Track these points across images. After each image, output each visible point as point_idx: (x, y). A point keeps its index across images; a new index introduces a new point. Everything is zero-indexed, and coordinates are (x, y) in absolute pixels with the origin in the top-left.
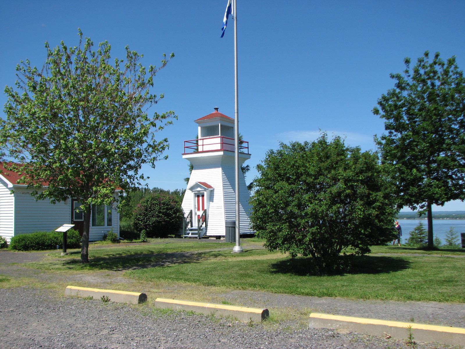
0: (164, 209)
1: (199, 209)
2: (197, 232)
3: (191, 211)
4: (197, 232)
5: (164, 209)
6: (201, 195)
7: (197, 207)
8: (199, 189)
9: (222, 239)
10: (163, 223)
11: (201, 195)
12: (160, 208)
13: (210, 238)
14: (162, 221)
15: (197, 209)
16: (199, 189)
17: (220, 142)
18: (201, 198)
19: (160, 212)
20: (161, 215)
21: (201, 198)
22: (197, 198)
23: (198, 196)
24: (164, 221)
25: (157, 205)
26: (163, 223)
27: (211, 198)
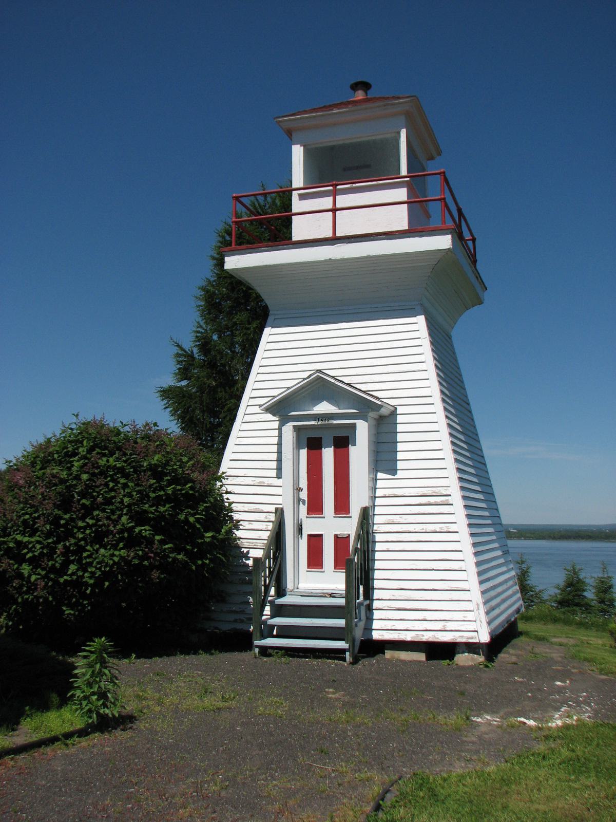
0: (158, 501)
1: (315, 507)
2: (341, 623)
3: (280, 513)
4: (341, 623)
5: (158, 501)
6: (328, 437)
7: (304, 495)
8: (324, 407)
9: (463, 659)
10: (155, 574)
11: (328, 437)
12: (144, 497)
13: (389, 654)
14: (152, 567)
15: (303, 509)
16: (324, 407)
17: (405, 199)
18: (328, 454)
19: (140, 518)
20: (145, 530)
21: (328, 454)
22: (304, 453)
23: (314, 445)
24: (164, 567)
25: (127, 476)
26: (155, 574)
27: (384, 458)
